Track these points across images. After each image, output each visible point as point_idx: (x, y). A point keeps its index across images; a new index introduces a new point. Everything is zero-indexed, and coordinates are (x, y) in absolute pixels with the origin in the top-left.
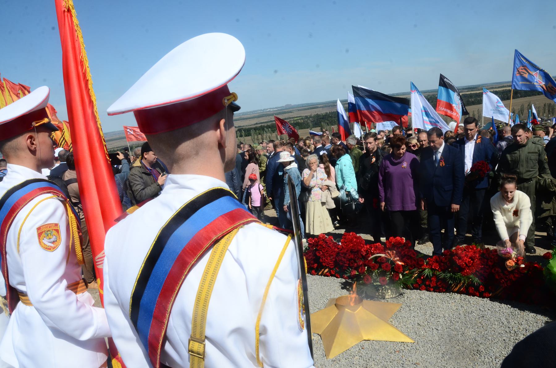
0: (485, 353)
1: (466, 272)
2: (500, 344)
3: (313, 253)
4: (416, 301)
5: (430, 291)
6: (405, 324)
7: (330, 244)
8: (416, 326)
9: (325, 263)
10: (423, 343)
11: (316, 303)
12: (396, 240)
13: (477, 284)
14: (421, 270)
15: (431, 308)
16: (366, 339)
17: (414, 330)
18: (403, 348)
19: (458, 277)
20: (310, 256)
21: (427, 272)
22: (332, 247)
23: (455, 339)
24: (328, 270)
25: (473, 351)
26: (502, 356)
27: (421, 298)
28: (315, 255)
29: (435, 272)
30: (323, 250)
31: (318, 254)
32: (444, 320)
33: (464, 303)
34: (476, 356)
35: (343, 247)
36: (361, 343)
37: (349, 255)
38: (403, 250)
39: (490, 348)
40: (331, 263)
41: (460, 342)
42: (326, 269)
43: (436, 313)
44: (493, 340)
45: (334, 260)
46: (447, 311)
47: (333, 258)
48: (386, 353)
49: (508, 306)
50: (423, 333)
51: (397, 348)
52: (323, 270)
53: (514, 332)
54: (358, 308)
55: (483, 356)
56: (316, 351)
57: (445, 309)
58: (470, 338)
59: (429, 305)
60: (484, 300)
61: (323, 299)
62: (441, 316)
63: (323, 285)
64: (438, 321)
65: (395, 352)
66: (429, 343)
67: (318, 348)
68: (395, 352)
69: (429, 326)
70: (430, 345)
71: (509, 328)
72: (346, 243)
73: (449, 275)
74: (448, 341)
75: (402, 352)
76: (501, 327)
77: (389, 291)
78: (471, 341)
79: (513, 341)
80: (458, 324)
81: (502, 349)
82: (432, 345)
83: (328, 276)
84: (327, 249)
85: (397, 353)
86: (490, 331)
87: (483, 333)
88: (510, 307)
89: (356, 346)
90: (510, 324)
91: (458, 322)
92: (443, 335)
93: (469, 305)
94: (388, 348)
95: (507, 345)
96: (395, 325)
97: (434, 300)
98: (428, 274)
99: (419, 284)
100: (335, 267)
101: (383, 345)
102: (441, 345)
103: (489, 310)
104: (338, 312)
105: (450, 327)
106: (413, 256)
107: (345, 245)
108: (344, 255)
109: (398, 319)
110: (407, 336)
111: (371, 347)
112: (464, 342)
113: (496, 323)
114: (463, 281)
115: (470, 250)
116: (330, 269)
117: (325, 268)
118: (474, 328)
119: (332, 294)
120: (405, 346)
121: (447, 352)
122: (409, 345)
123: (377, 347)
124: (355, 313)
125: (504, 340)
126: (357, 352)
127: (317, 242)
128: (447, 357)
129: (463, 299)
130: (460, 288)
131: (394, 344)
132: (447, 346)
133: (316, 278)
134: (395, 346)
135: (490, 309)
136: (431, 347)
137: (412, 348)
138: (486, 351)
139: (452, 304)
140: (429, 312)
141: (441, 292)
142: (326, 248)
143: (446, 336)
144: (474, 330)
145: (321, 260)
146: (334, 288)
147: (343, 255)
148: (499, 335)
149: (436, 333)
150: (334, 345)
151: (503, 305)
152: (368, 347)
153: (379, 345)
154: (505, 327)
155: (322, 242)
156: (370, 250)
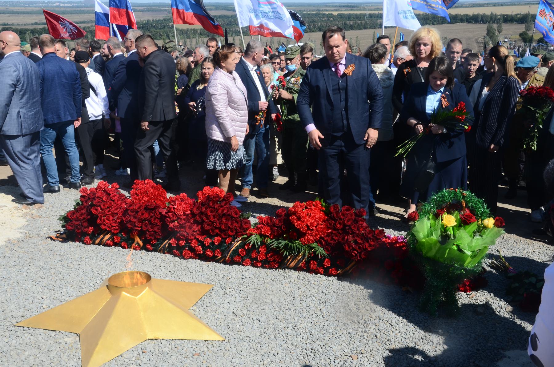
0: (321, 352)
1: (308, 240)
2: (344, 339)
3: (87, 211)
4: (235, 280)
5: (257, 267)
6: (214, 313)
7: (114, 196)
8: (231, 316)
9: (105, 225)
10: (236, 340)
11: (83, 286)
12: (213, 191)
13: (321, 255)
14: (245, 236)
15: (255, 290)
16: (152, 338)
17: (226, 322)
18: (206, 349)
19: (296, 246)
20: (82, 214)
21: (255, 239)
22: (118, 201)
23: (283, 334)
24: (110, 236)
25: (306, 349)
26: (344, 355)
27: (243, 277)
28: (90, 213)
29: (264, 240)
30: (102, 206)
31: (94, 211)
32: (271, 308)
33: (302, 284)
34: (309, 357)
35: (133, 201)
36: (143, 343)
37: (143, 214)
38: (222, 206)
39: (330, 345)
40: (115, 225)
41: (289, 337)
42: (107, 234)
43: (261, 298)
44: (334, 333)
45: (119, 220)
46: (277, 295)
47: (118, 218)
48: (180, 357)
49: (360, 286)
50: (238, 326)
51: (196, 350)
52: (102, 236)
53: (364, 322)
54: (144, 290)
55: (318, 356)
56: (67, 360)
57: (274, 292)
58: (304, 331)
59: (253, 286)
60: (330, 279)
61: (95, 279)
62: (268, 301)
63: (100, 259)
64: (262, 308)
65: (193, 355)
66: (245, 340)
67: (72, 356)
68: (193, 355)
69: (249, 316)
70: (246, 344)
71: (358, 316)
72: (138, 195)
73: (283, 243)
74: (272, 337)
75: (203, 355)
76: (348, 315)
78: (305, 336)
79: (361, 334)
80: (290, 311)
81: (345, 345)
82: (250, 343)
83: (109, 245)
84: (108, 203)
85: (196, 357)
86: (332, 322)
87: (322, 324)
88: (363, 288)
89: (134, 349)
90: (360, 311)
91: (290, 310)
92: (267, 329)
93: (308, 286)
94: (184, 351)
95: (353, 339)
96: (200, 316)
97: (261, 279)
98: (254, 242)
99: (242, 257)
100: (120, 232)
101: (176, 346)
102: (262, 343)
103: (334, 292)
104: (111, 297)
105: (278, 317)
106: (235, 216)
107: (136, 199)
108: (134, 213)
109: (205, 306)
110: (214, 332)
111: (157, 350)
112: (295, 337)
113: (342, 310)
114: (302, 252)
115: (313, 208)
116: (113, 234)
117: (105, 233)
118: (310, 317)
119: (111, 271)
120: (210, 346)
121: (269, 353)
122: (215, 345)
123: (166, 350)
124: (137, 298)
125: (349, 333)
126: (134, 359)
127: (94, 194)
128: (269, 360)
129: (301, 278)
130: (299, 262)
131: (194, 344)
132: (269, 345)
133: (91, 248)
134: (194, 347)
135: (337, 291)
136: (247, 346)
137: (219, 349)
138: (324, 350)
139: (286, 285)
140: (252, 296)
141: (273, 269)
142: (107, 202)
143: (272, 329)
144: (311, 321)
145: (98, 221)
146: (116, 263)
147: (133, 214)
148: (344, 327)
149: (258, 325)
150: (97, 349)
151: (354, 285)
152: (153, 350)
153: (170, 346)
154: (353, 316)
155: (102, 194)
156: (172, 205)
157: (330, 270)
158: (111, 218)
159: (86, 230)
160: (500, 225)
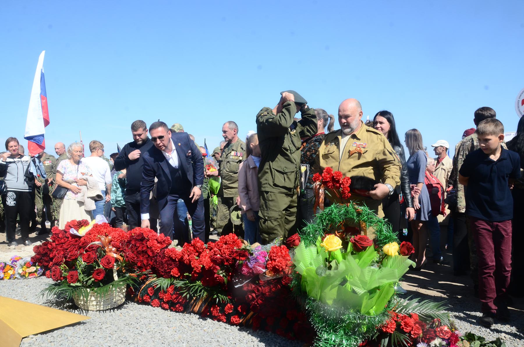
77: (93, 298)
99: (151, 297)
141: (178, 312)
157: (232, 317)
159: (46, 264)
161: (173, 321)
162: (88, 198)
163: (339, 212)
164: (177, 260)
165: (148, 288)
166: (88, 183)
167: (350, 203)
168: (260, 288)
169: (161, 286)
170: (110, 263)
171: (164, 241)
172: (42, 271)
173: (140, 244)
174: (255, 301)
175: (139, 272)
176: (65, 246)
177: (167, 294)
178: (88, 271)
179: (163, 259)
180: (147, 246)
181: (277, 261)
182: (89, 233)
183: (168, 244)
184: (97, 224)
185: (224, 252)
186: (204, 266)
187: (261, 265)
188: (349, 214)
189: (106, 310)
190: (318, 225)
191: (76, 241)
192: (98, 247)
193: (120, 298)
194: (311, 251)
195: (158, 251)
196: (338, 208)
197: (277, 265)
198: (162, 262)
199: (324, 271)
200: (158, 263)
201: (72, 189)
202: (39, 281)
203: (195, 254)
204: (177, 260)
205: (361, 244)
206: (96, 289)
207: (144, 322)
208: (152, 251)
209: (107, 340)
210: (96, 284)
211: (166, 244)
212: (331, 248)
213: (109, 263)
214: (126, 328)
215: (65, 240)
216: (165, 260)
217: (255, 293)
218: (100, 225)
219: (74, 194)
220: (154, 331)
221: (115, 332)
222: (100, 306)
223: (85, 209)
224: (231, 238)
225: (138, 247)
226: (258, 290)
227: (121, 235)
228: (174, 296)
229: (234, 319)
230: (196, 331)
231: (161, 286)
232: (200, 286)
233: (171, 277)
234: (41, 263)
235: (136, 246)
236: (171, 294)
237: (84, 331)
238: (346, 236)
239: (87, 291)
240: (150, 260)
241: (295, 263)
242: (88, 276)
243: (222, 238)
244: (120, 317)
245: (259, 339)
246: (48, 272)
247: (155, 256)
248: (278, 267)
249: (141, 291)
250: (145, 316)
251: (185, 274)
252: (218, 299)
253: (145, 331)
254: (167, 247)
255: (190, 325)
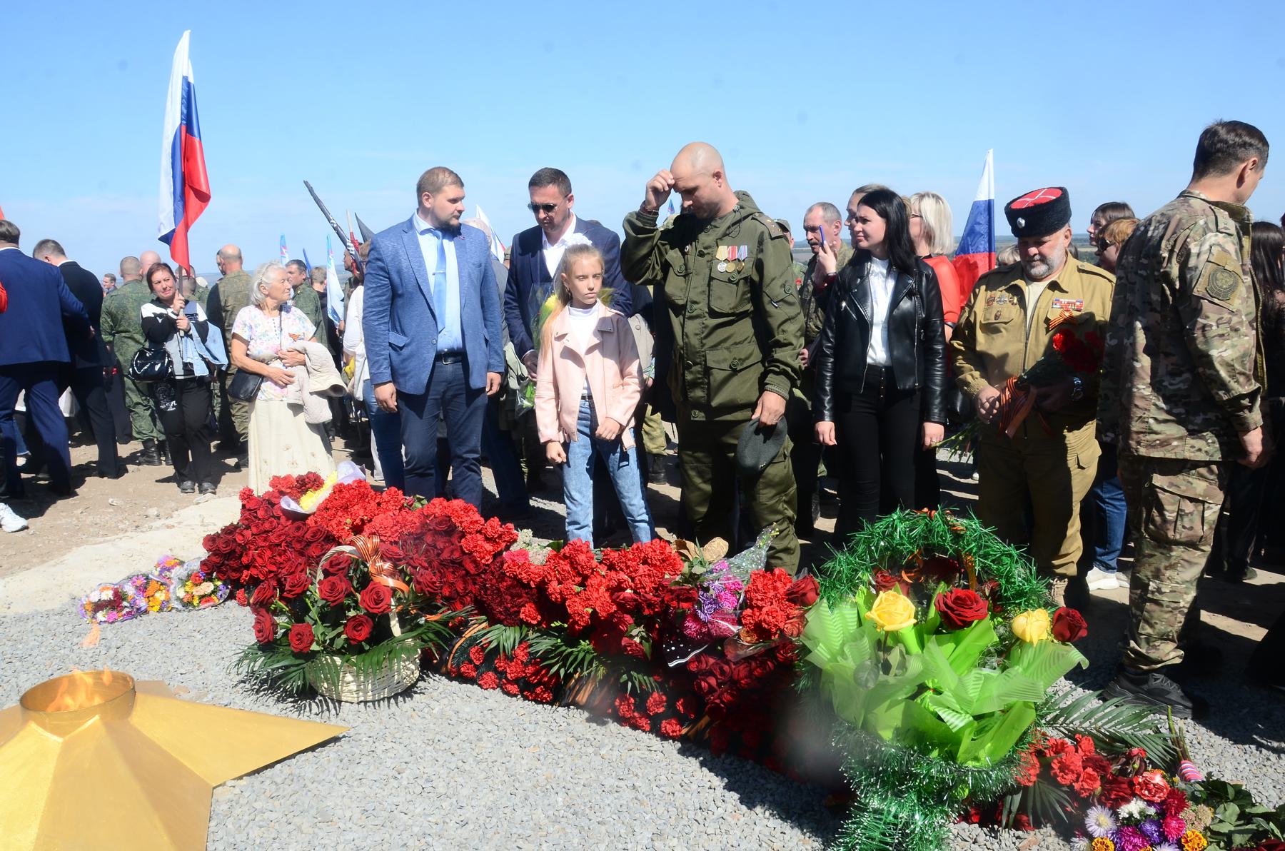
9: (255, 567)
77: (349, 678)
99: (477, 668)
142: (264, 520)
157: (664, 722)
158: (268, 554)
159: (234, 575)
160: (1068, 634)
161: (531, 727)
162: (311, 394)
163: (911, 531)
164: (533, 586)
165: (470, 646)
166: (307, 360)
167: (937, 509)
168: (726, 668)
169: (498, 645)
170: (382, 600)
171: (500, 537)
172: (228, 591)
173: (445, 542)
174: (716, 694)
175: (448, 610)
176: (273, 538)
177: (513, 663)
178: (332, 616)
179: (501, 582)
180: (461, 547)
181: (764, 610)
182: (325, 507)
183: (508, 542)
184: (341, 484)
185: (641, 583)
186: (595, 612)
187: (727, 617)
188: (933, 536)
189: (379, 701)
190: (861, 558)
191: (298, 528)
192: (351, 561)
193: (409, 672)
194: (843, 616)
195: (487, 560)
196: (908, 520)
197: (765, 621)
198: (498, 589)
199: (873, 676)
200: (489, 592)
201: (271, 375)
202: (222, 615)
203: (574, 581)
204: (533, 586)
205: (959, 615)
206: (355, 657)
207: (466, 735)
208: (475, 562)
209: (390, 786)
210: (353, 648)
211: (505, 541)
212: (889, 624)
213: (378, 601)
214: (428, 754)
215: (271, 523)
216: (505, 584)
217: (717, 678)
218: (349, 487)
219: (277, 388)
220: (490, 760)
221: (404, 766)
222: (366, 692)
223: (308, 420)
224: (658, 552)
225: (442, 550)
226: (722, 672)
227: (400, 521)
228: (530, 669)
229: (668, 726)
230: (584, 757)
231: (498, 645)
232: (587, 652)
233: (521, 623)
234: (224, 573)
235: (436, 548)
236: (522, 662)
237: (338, 763)
238: (926, 581)
239: (334, 661)
240: (470, 581)
241: (808, 644)
242: (334, 626)
243: (637, 549)
244: (413, 721)
245: (726, 780)
246: (240, 593)
247: (482, 573)
248: (766, 626)
249: (454, 651)
250: (468, 718)
251: (553, 625)
252: (630, 684)
253: (471, 760)
254: (507, 548)
255: (570, 739)
